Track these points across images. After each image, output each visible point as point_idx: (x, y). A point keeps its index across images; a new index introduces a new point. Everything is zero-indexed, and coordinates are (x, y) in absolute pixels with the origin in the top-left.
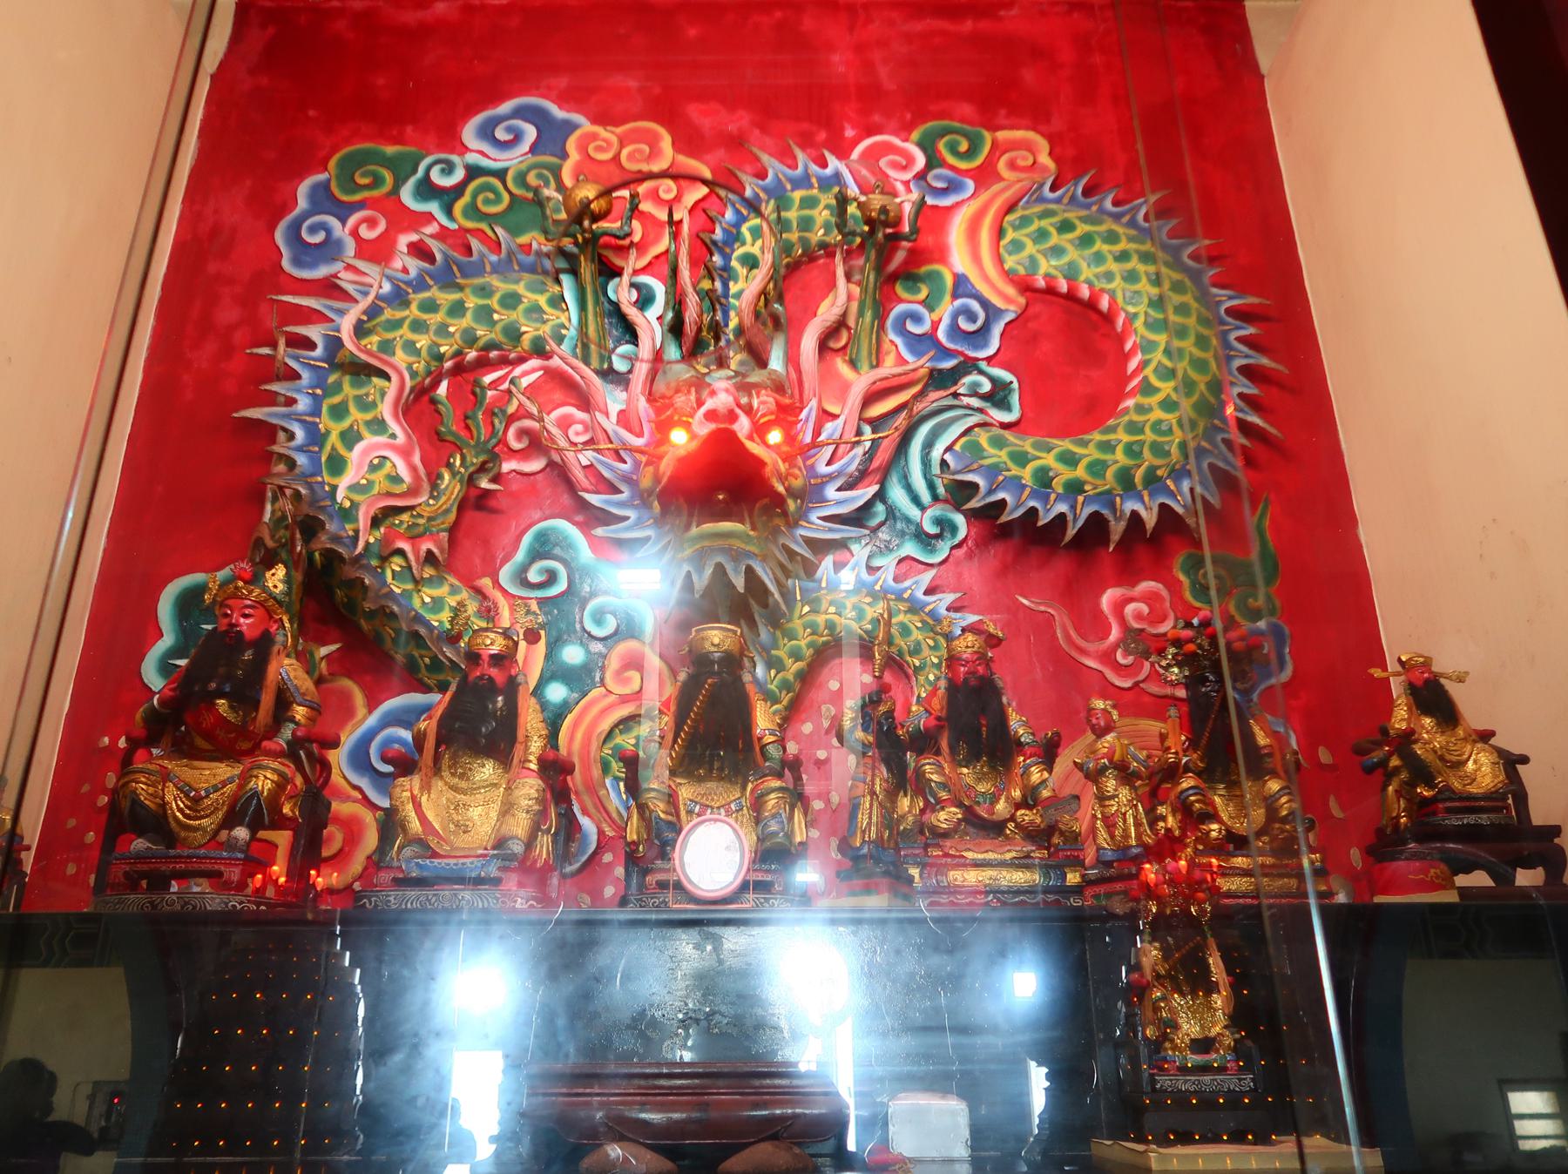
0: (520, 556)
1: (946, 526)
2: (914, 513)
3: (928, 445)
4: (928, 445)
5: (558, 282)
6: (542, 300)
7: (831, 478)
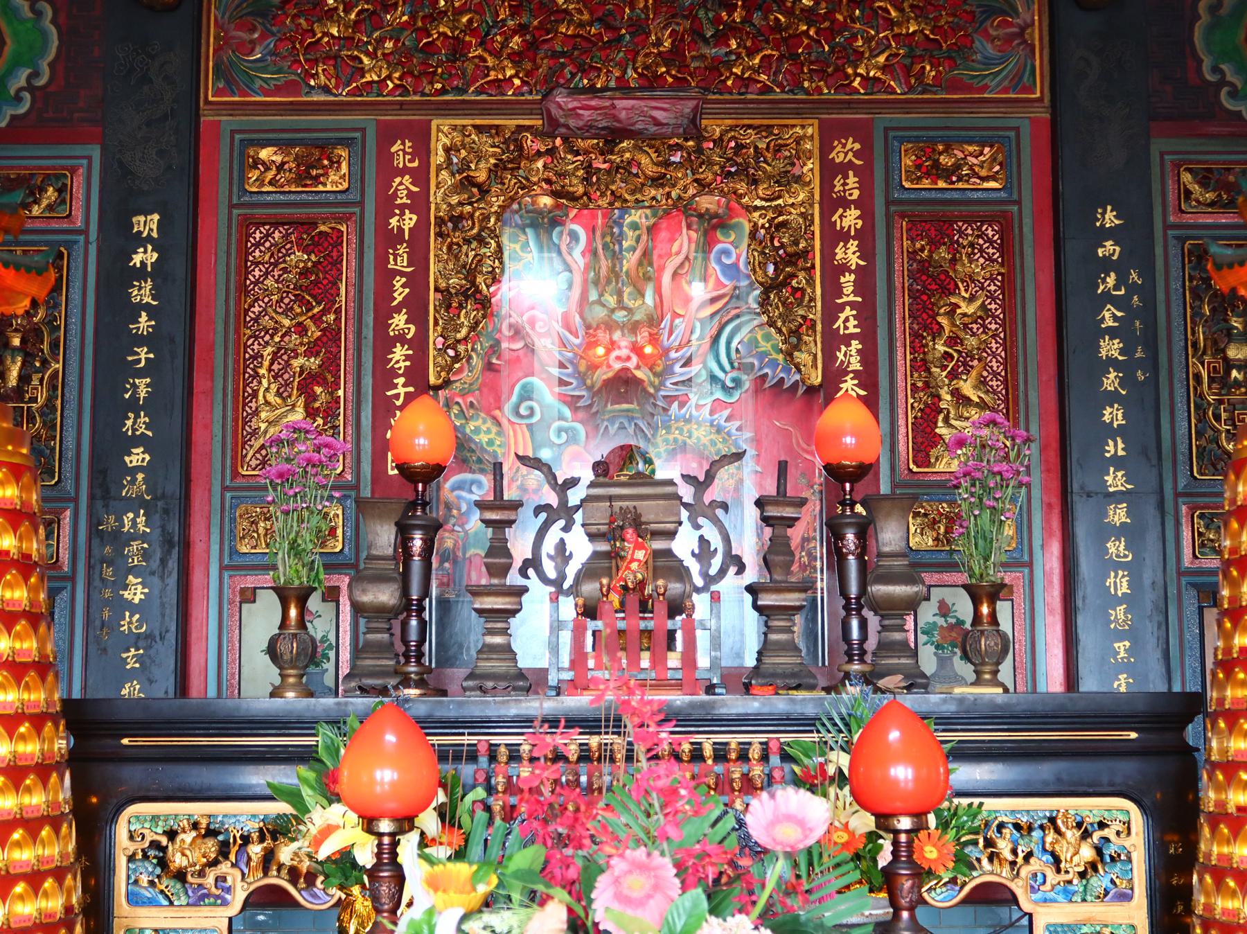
0: (514, 398)
1: (738, 382)
2: (721, 375)
3: (729, 343)
4: (729, 343)
5: (525, 233)
6: (518, 247)
7: (677, 360)
